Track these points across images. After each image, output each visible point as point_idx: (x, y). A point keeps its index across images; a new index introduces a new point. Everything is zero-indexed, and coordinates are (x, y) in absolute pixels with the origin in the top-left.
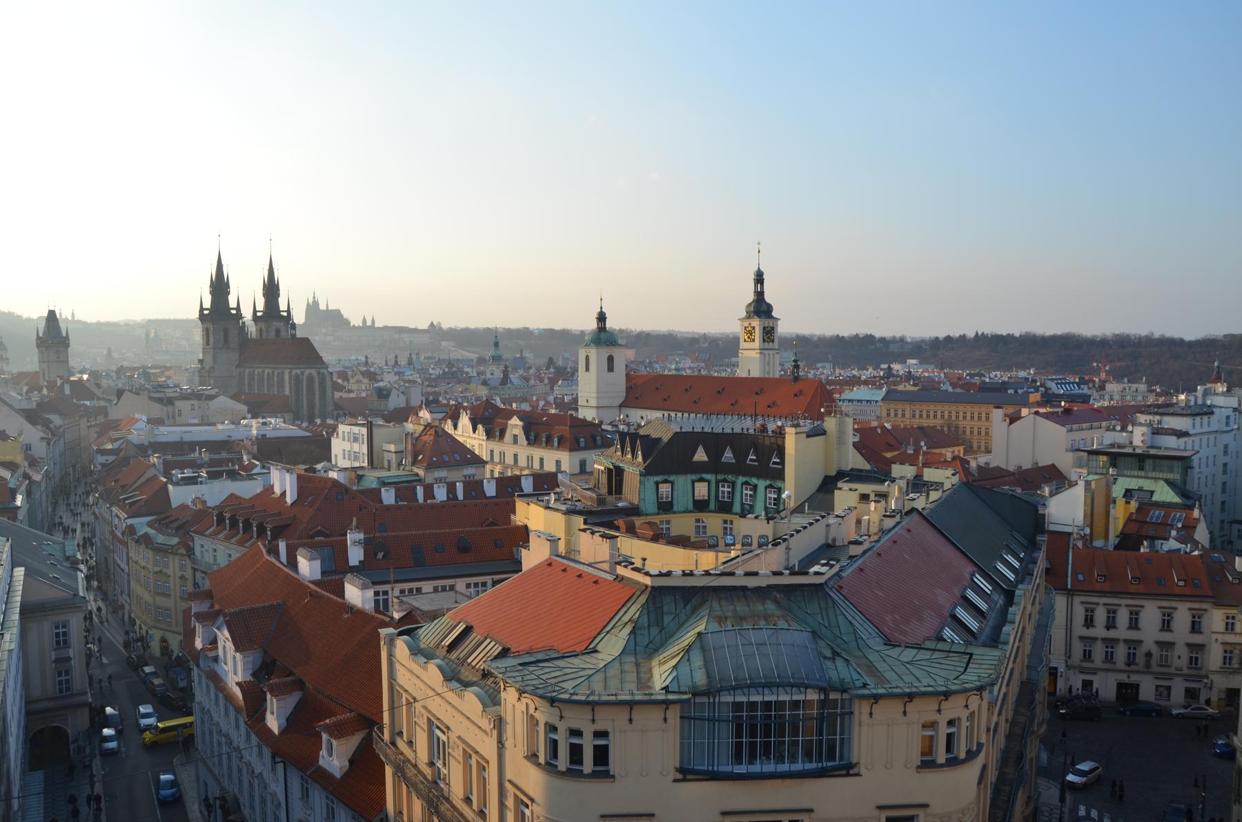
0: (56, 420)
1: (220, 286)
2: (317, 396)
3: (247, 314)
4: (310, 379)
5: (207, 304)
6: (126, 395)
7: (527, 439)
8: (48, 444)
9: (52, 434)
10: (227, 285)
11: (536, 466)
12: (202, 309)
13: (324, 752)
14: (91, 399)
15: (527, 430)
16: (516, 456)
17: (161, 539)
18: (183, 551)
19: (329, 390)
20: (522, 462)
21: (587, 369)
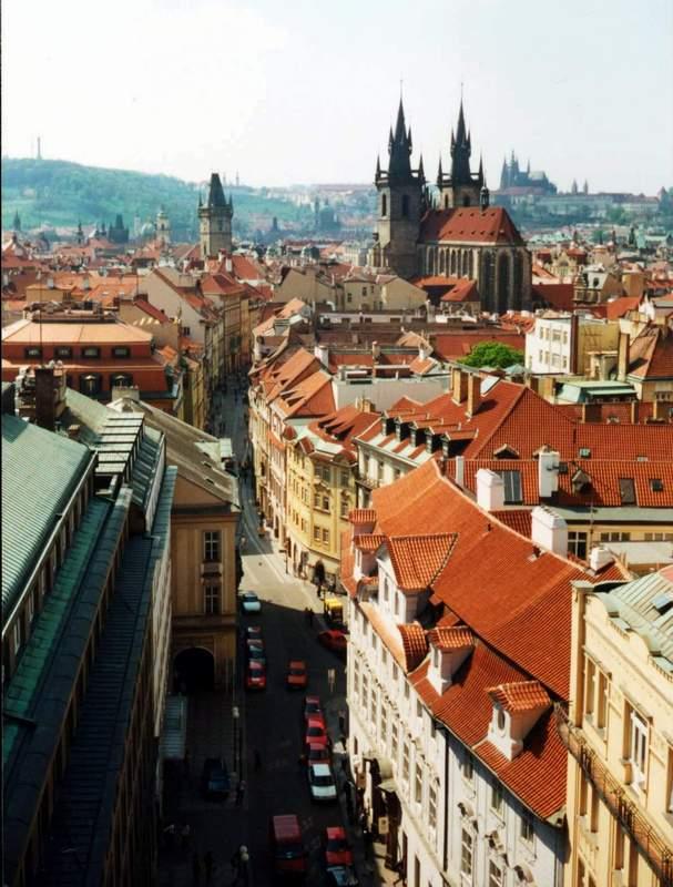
1: (401, 144)
3: (431, 177)
4: (504, 259)
5: (385, 166)
6: (291, 274)
8: (207, 328)
9: (210, 317)
10: (408, 142)
13: (493, 725)
14: (254, 278)
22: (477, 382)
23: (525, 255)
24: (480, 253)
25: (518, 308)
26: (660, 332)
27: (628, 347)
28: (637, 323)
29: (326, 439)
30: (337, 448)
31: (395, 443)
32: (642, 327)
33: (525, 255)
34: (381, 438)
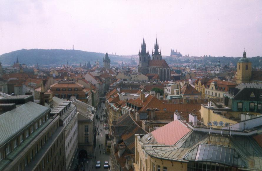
0: (103, 79)
1: (144, 46)
2: (166, 75)
3: (150, 53)
4: (165, 70)
5: (140, 51)
7: (216, 88)
11: (218, 96)
12: (139, 52)
14: (113, 74)
15: (216, 86)
16: (212, 93)
17: (115, 108)
18: (119, 112)
19: (169, 74)
20: (214, 95)
21: (239, 69)
22: (144, 95)
23: (169, 69)
24: (160, 69)
25: (168, 80)
26: (188, 85)
27: (181, 89)
28: (183, 83)
29: (116, 107)
30: (119, 109)
31: (128, 108)
32: (184, 84)
33: (169, 69)
34: (126, 107)
